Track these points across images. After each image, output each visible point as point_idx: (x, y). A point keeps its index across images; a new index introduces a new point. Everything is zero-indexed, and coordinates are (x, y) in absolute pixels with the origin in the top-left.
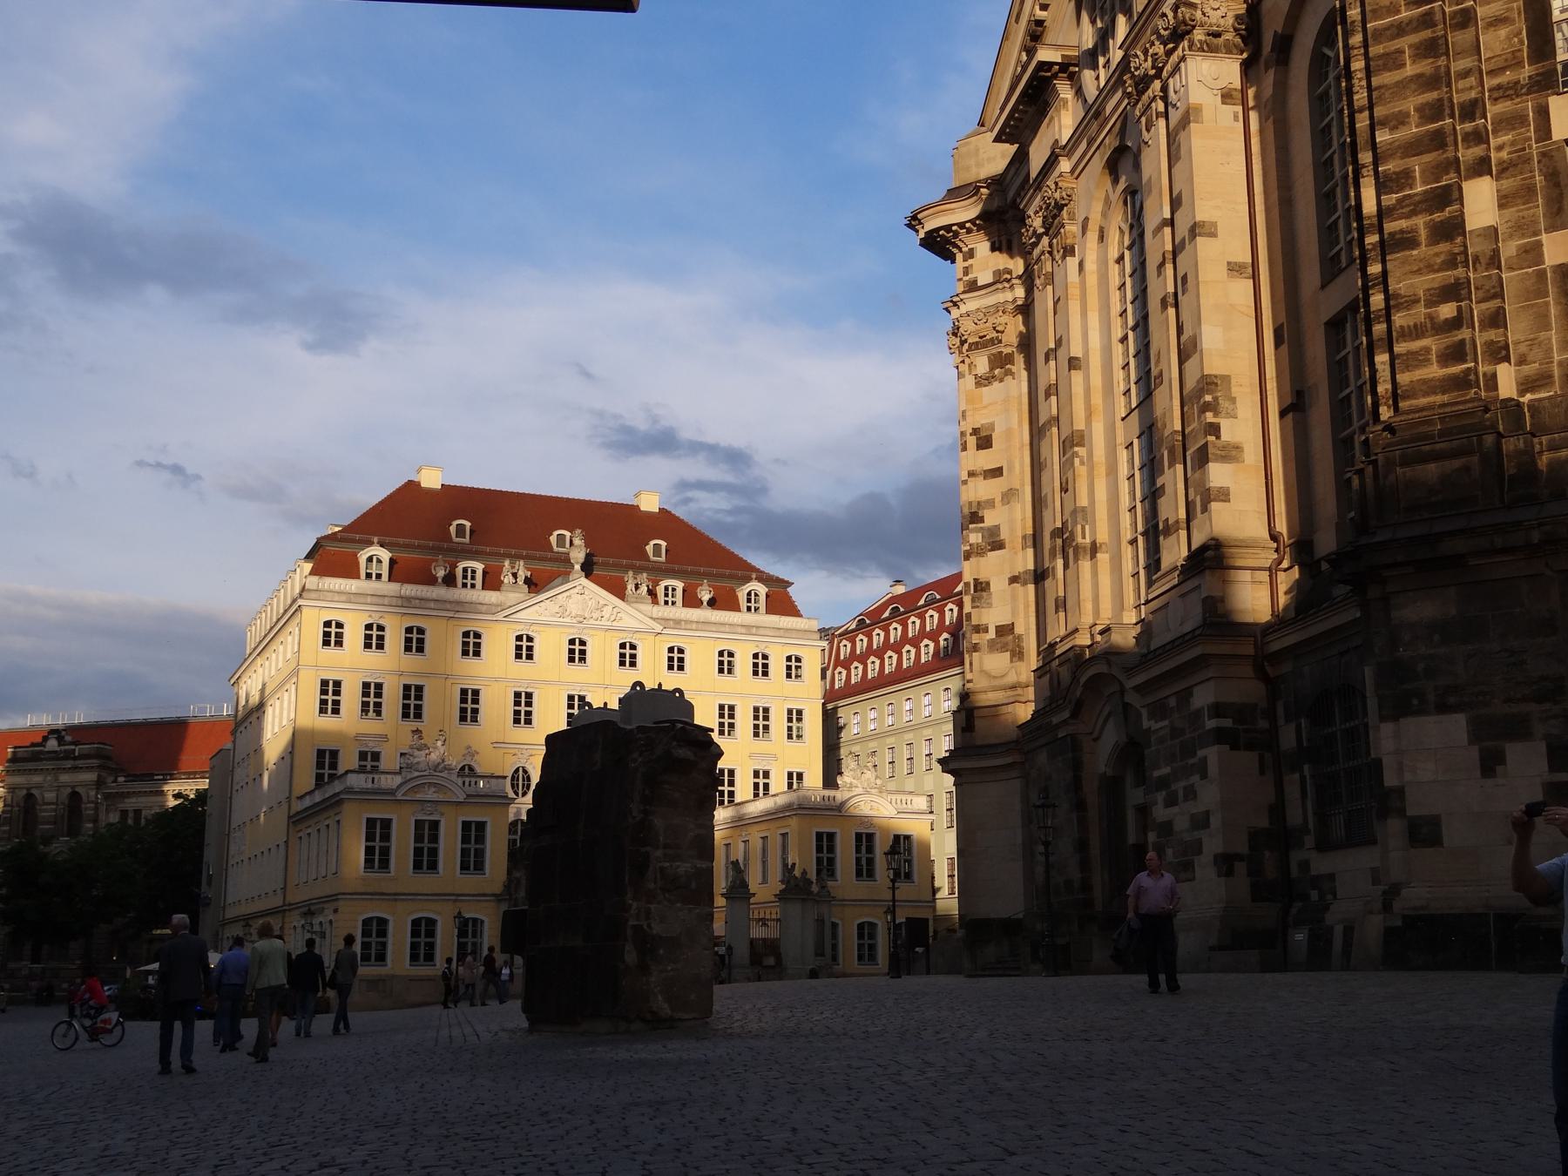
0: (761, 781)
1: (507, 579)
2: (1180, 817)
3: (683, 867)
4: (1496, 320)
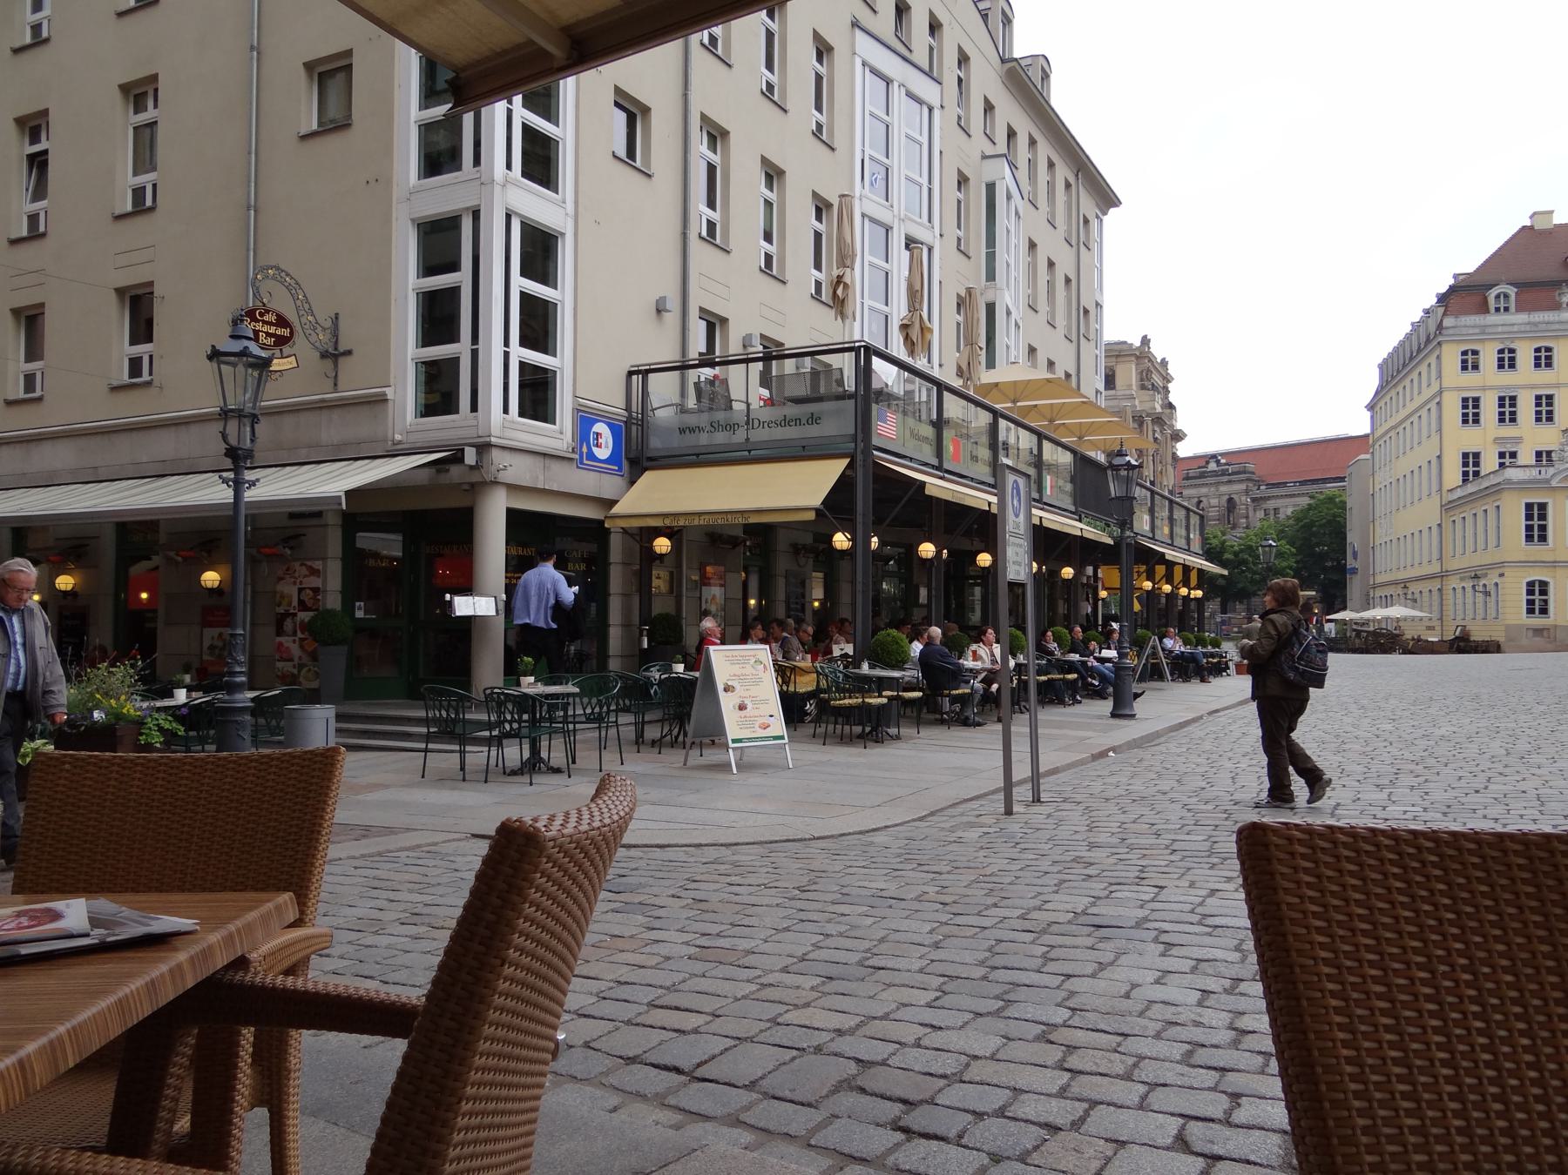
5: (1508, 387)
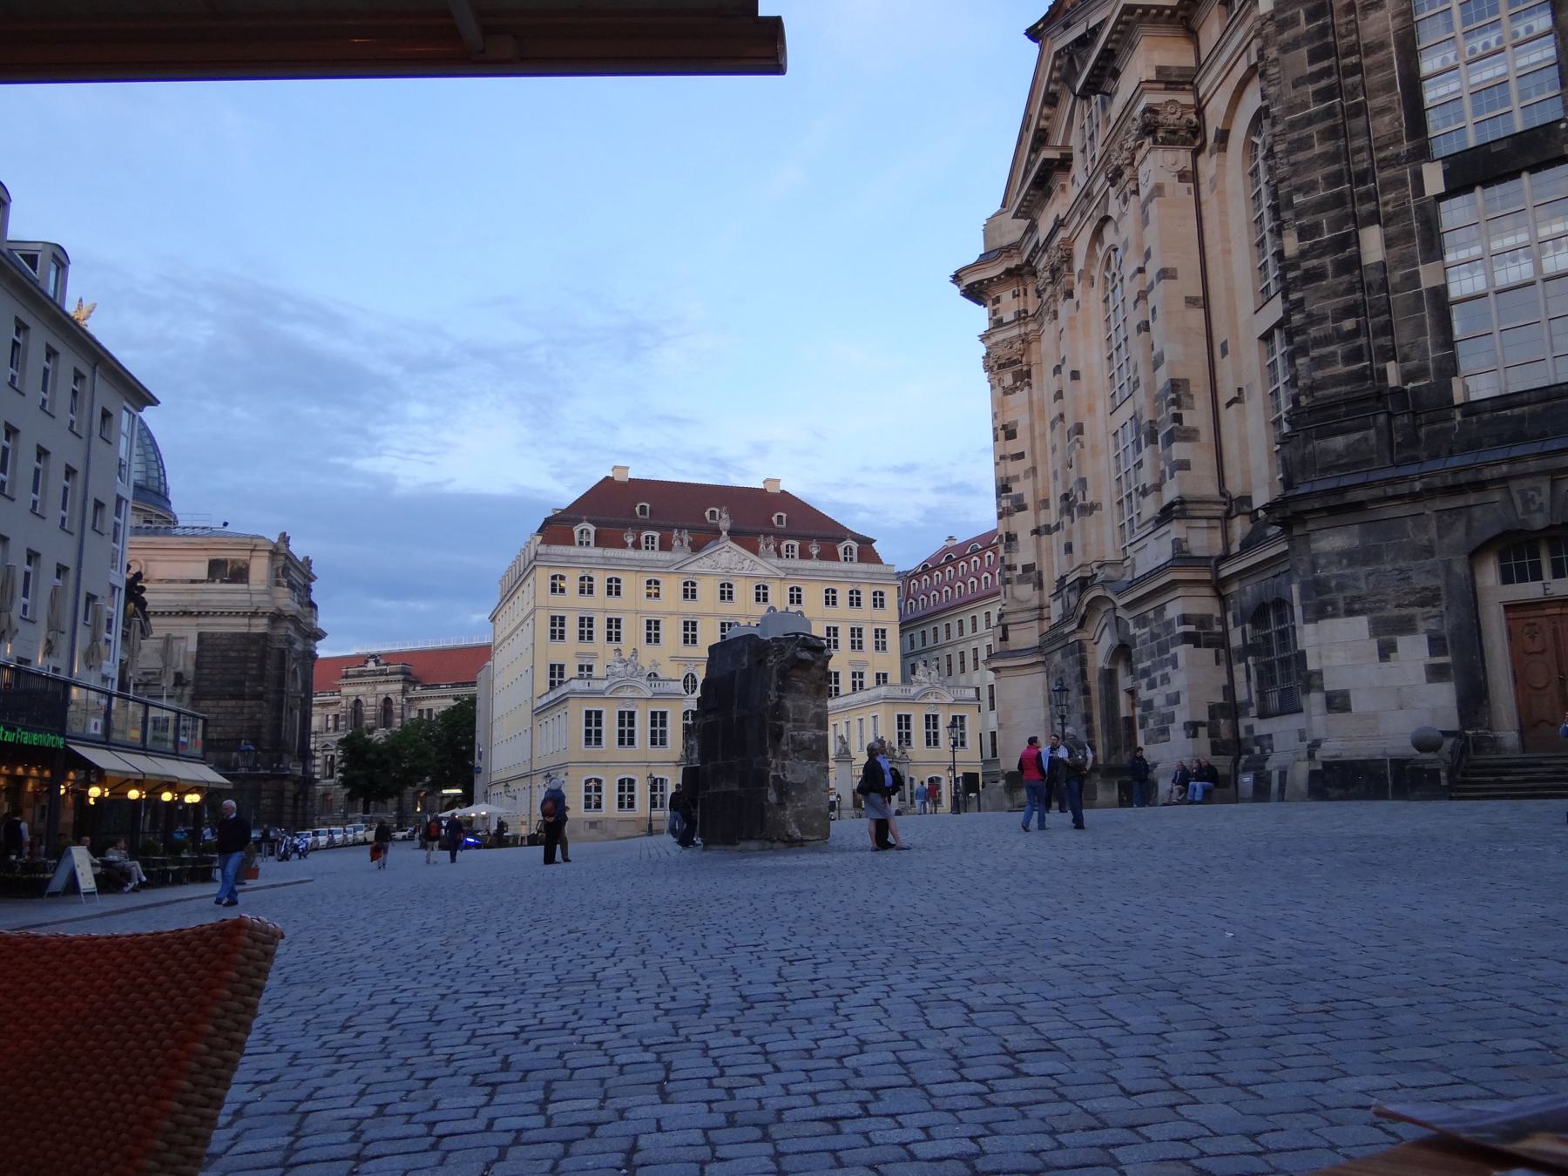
0: (858, 680)
1: (676, 543)
2: (1158, 697)
3: (807, 735)
4: (1387, 329)
5: (586, 610)
